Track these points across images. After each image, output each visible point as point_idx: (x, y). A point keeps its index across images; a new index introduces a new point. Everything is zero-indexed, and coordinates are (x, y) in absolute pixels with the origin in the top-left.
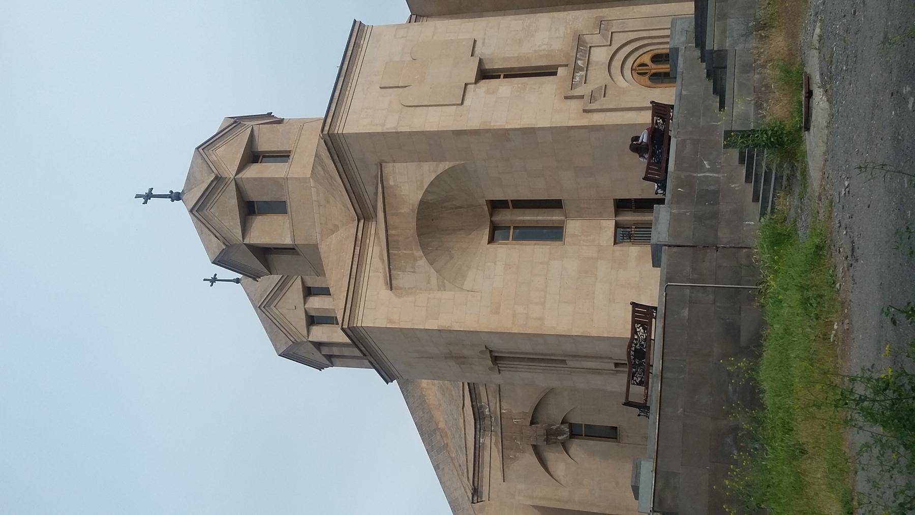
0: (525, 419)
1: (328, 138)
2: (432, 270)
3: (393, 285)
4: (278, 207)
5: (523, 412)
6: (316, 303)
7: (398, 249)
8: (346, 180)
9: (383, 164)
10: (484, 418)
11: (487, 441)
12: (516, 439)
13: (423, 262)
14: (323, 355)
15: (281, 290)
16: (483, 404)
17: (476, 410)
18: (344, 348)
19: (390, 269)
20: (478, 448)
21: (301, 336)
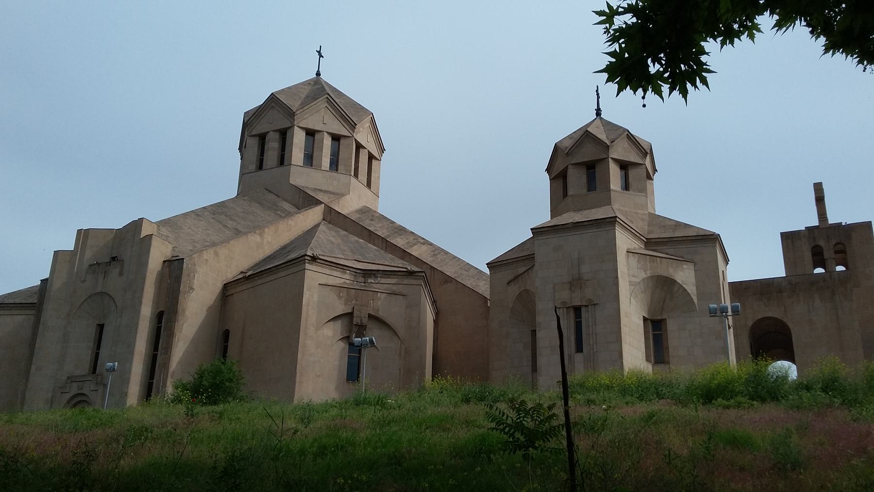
0: (373, 310)
1: (715, 237)
2: (638, 280)
3: (629, 254)
4: (626, 187)
5: (379, 310)
6: (327, 142)
7: (650, 262)
8: (680, 239)
9: (693, 264)
10: (365, 278)
11: (347, 277)
12: (357, 300)
13: (643, 275)
14: (269, 132)
15: (340, 116)
16: (379, 279)
17: (374, 273)
18: (277, 152)
19: (638, 253)
20: (343, 268)
21: (299, 120)
